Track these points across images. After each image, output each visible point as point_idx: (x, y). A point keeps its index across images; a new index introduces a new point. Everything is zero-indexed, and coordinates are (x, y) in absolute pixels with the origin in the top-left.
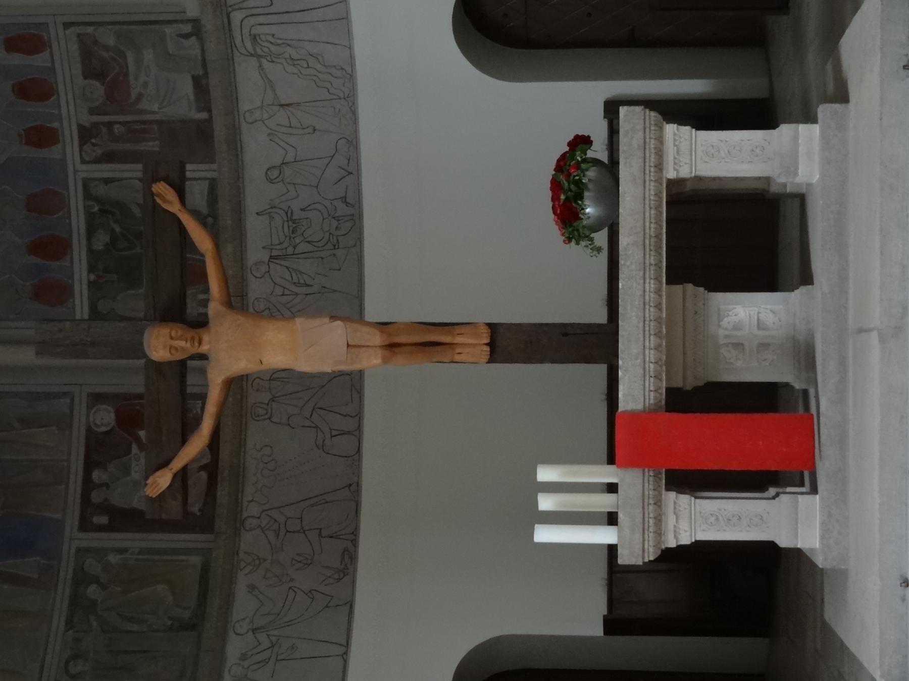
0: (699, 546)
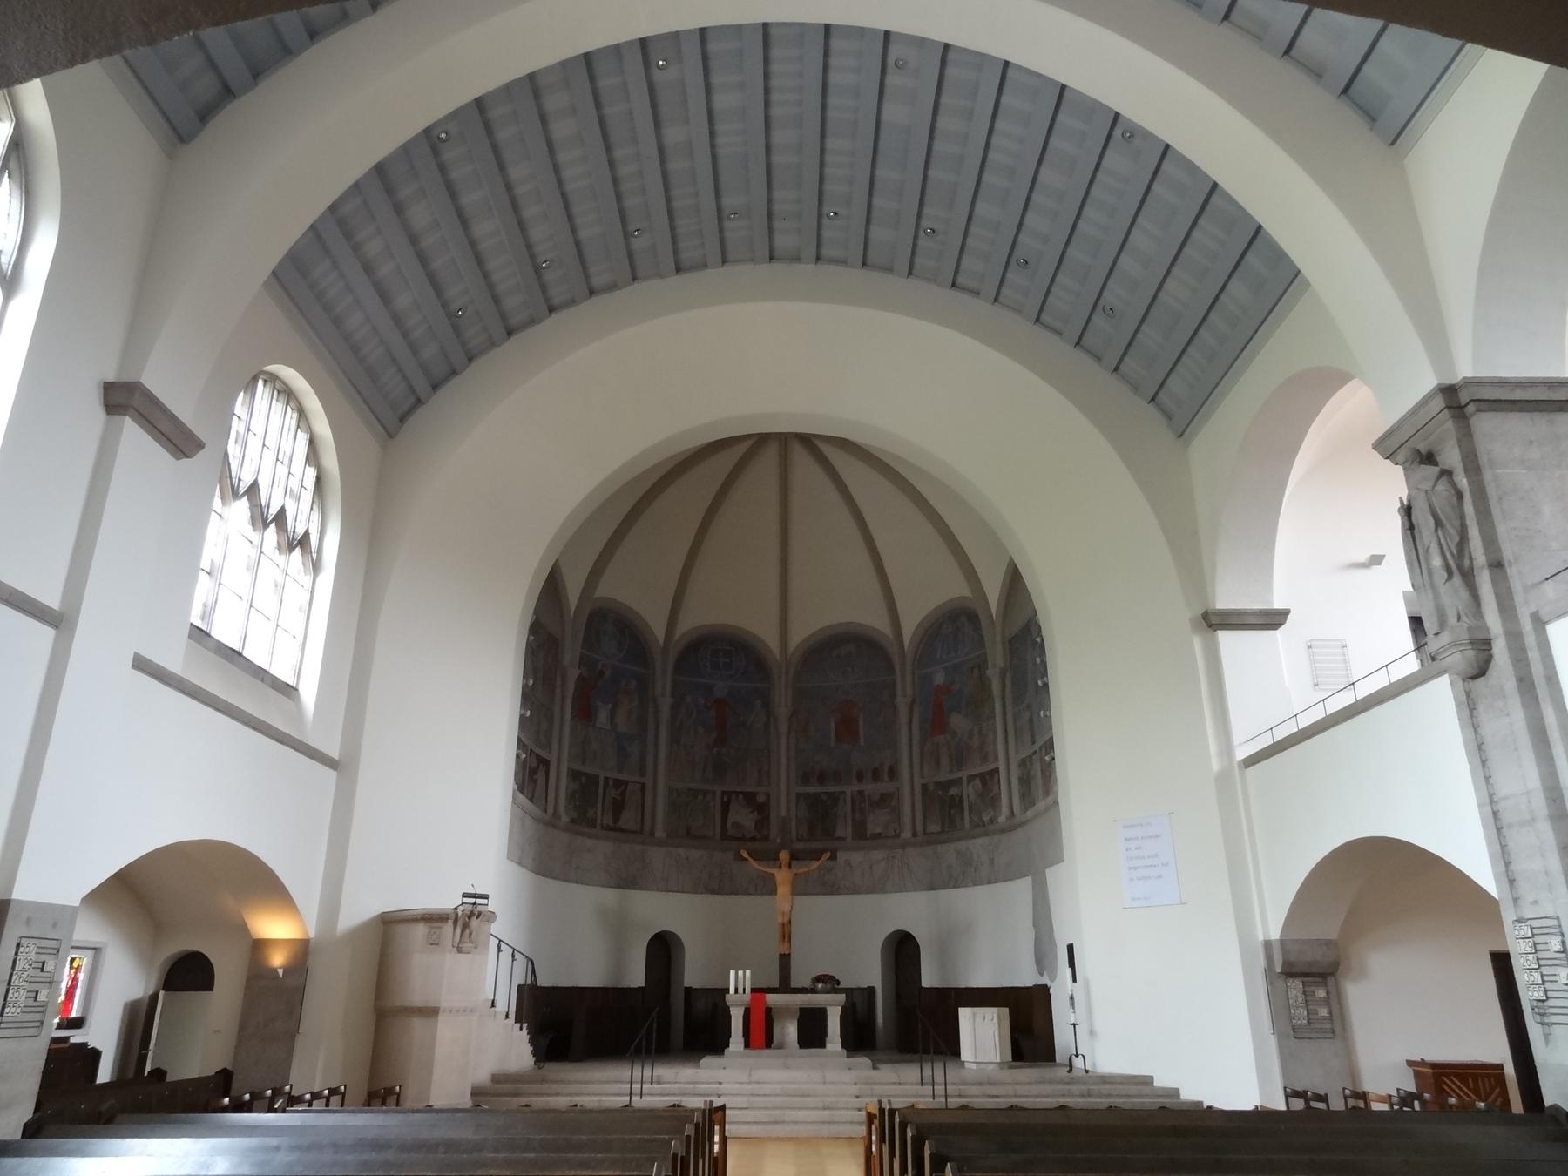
0: (730, 1017)
